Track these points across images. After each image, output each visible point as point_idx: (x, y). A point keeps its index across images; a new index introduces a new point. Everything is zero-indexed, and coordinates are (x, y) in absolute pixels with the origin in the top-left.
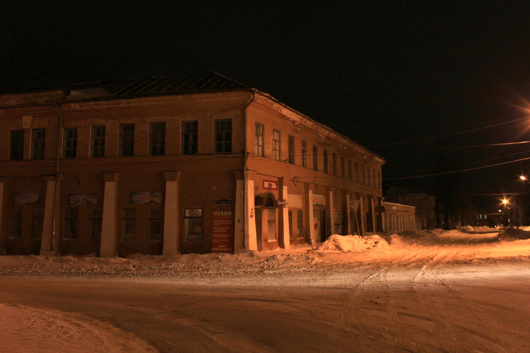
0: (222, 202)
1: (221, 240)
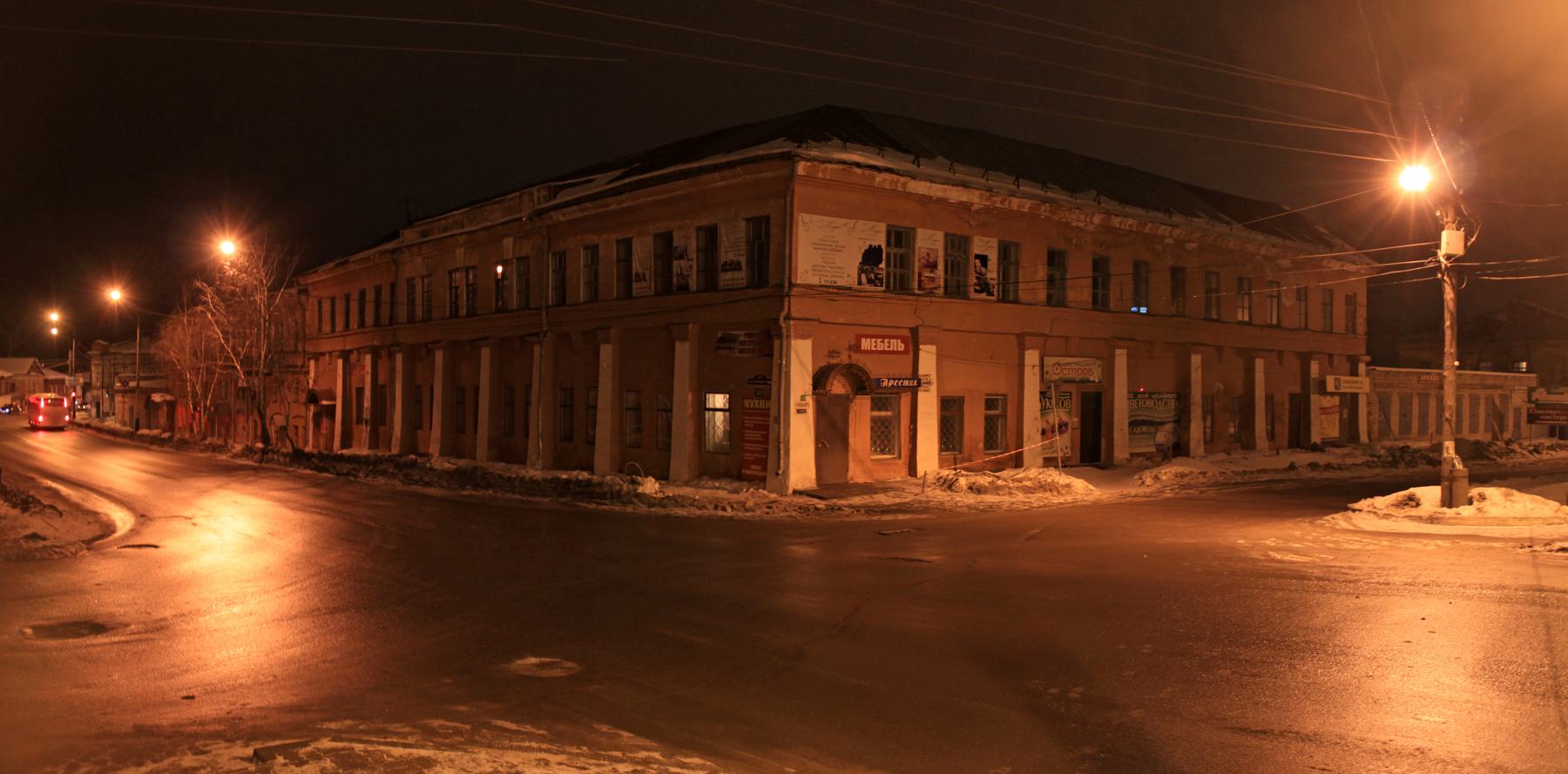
0: (757, 382)
1: (755, 455)
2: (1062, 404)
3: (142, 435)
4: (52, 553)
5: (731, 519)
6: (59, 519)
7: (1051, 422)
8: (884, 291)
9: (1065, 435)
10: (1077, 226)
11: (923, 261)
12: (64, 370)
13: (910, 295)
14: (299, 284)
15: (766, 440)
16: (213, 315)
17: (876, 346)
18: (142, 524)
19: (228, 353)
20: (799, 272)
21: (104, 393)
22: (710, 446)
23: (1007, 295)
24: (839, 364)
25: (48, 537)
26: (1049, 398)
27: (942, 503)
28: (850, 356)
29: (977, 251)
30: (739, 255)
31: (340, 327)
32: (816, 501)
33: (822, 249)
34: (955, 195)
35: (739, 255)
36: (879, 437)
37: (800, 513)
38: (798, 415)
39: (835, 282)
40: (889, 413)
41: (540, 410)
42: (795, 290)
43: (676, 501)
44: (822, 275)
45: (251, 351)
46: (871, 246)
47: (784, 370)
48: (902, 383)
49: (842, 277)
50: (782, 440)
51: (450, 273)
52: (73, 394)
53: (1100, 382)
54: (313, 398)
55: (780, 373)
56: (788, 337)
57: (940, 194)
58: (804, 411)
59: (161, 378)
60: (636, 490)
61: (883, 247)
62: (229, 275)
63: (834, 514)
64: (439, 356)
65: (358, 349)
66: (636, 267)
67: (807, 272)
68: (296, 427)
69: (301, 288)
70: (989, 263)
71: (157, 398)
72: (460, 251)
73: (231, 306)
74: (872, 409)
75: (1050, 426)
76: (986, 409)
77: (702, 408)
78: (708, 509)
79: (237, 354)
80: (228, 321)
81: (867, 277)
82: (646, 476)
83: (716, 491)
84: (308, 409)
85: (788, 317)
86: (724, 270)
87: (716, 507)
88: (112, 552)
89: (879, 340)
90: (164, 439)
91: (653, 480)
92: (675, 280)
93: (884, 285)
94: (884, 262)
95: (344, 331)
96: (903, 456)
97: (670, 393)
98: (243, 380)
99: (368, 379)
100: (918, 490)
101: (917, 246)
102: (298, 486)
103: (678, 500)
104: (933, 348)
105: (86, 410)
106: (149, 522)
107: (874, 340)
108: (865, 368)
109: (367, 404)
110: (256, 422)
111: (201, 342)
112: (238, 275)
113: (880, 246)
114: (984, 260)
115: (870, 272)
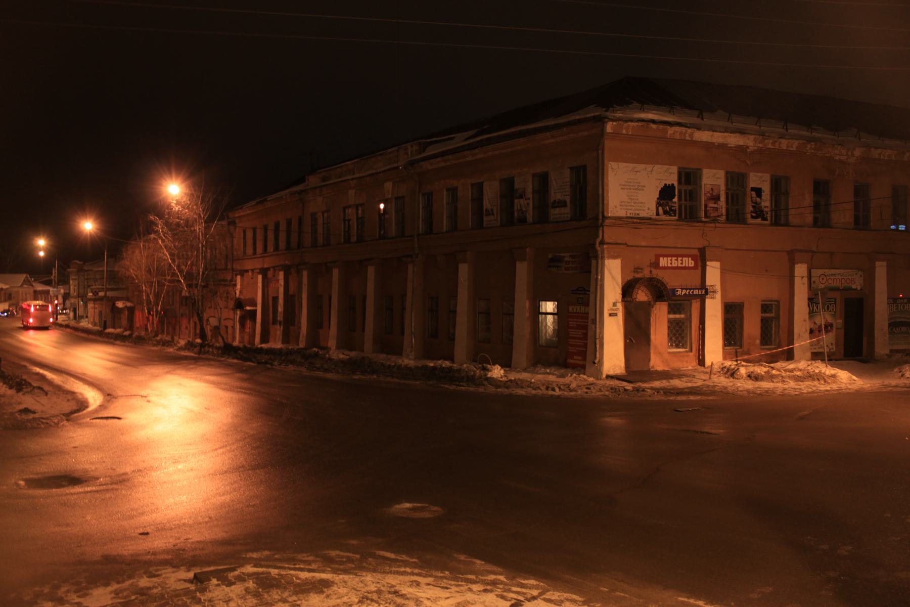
0: (579, 292)
1: (577, 348)
2: (828, 307)
3: (109, 333)
4: (40, 423)
5: (559, 397)
6: (45, 397)
7: (818, 322)
9: (831, 333)
10: (840, 159)
11: (708, 194)
12: (48, 283)
13: (698, 222)
14: (228, 218)
15: (586, 335)
16: (163, 241)
17: (671, 264)
18: (108, 401)
19: (174, 270)
20: (609, 207)
21: (79, 300)
22: (542, 341)
23: (779, 218)
24: (642, 278)
25: (36, 411)
26: (816, 304)
27: (726, 388)
28: (651, 271)
29: (752, 184)
30: (564, 195)
31: (260, 250)
32: (625, 384)
33: (627, 189)
34: (734, 140)
35: (564, 195)
36: (675, 335)
37: (612, 392)
38: (610, 317)
39: (638, 214)
40: (683, 316)
41: (413, 314)
42: (607, 222)
43: (517, 383)
44: (629, 209)
45: (192, 268)
46: (665, 185)
47: (599, 283)
48: (693, 292)
49: (644, 210)
50: (597, 337)
51: (344, 209)
52: (56, 302)
53: (861, 289)
54: (239, 304)
55: (596, 285)
56: (603, 258)
57: (721, 141)
58: (616, 315)
59: (123, 289)
60: (486, 375)
61: (676, 185)
62: (175, 211)
63: (639, 394)
64: (336, 273)
65: (274, 267)
66: (487, 204)
67: (616, 207)
68: (227, 327)
69: (231, 220)
70: (763, 194)
71: (120, 304)
72: (351, 193)
73: (176, 234)
74: (669, 313)
75: (817, 327)
76: (762, 313)
77: (536, 312)
78: (541, 390)
79: (181, 271)
80: (174, 246)
81: (663, 209)
82: (494, 364)
83: (547, 376)
84: (235, 313)
85: (602, 243)
86: (554, 207)
87: (547, 388)
88: (86, 423)
89: (674, 259)
90: (125, 336)
91: (499, 367)
92: (516, 214)
93: (677, 215)
94: (676, 197)
95: (263, 253)
96: (694, 350)
97: (512, 300)
98: (186, 291)
99: (281, 290)
100: (706, 377)
101: (703, 183)
102: (227, 372)
103: (519, 383)
104: (717, 264)
105: (65, 314)
106: (114, 400)
107: (669, 259)
108: (664, 281)
109: (280, 309)
110: (195, 323)
111: (154, 261)
112: (182, 210)
113: (673, 184)
114: (758, 191)
115: (666, 206)
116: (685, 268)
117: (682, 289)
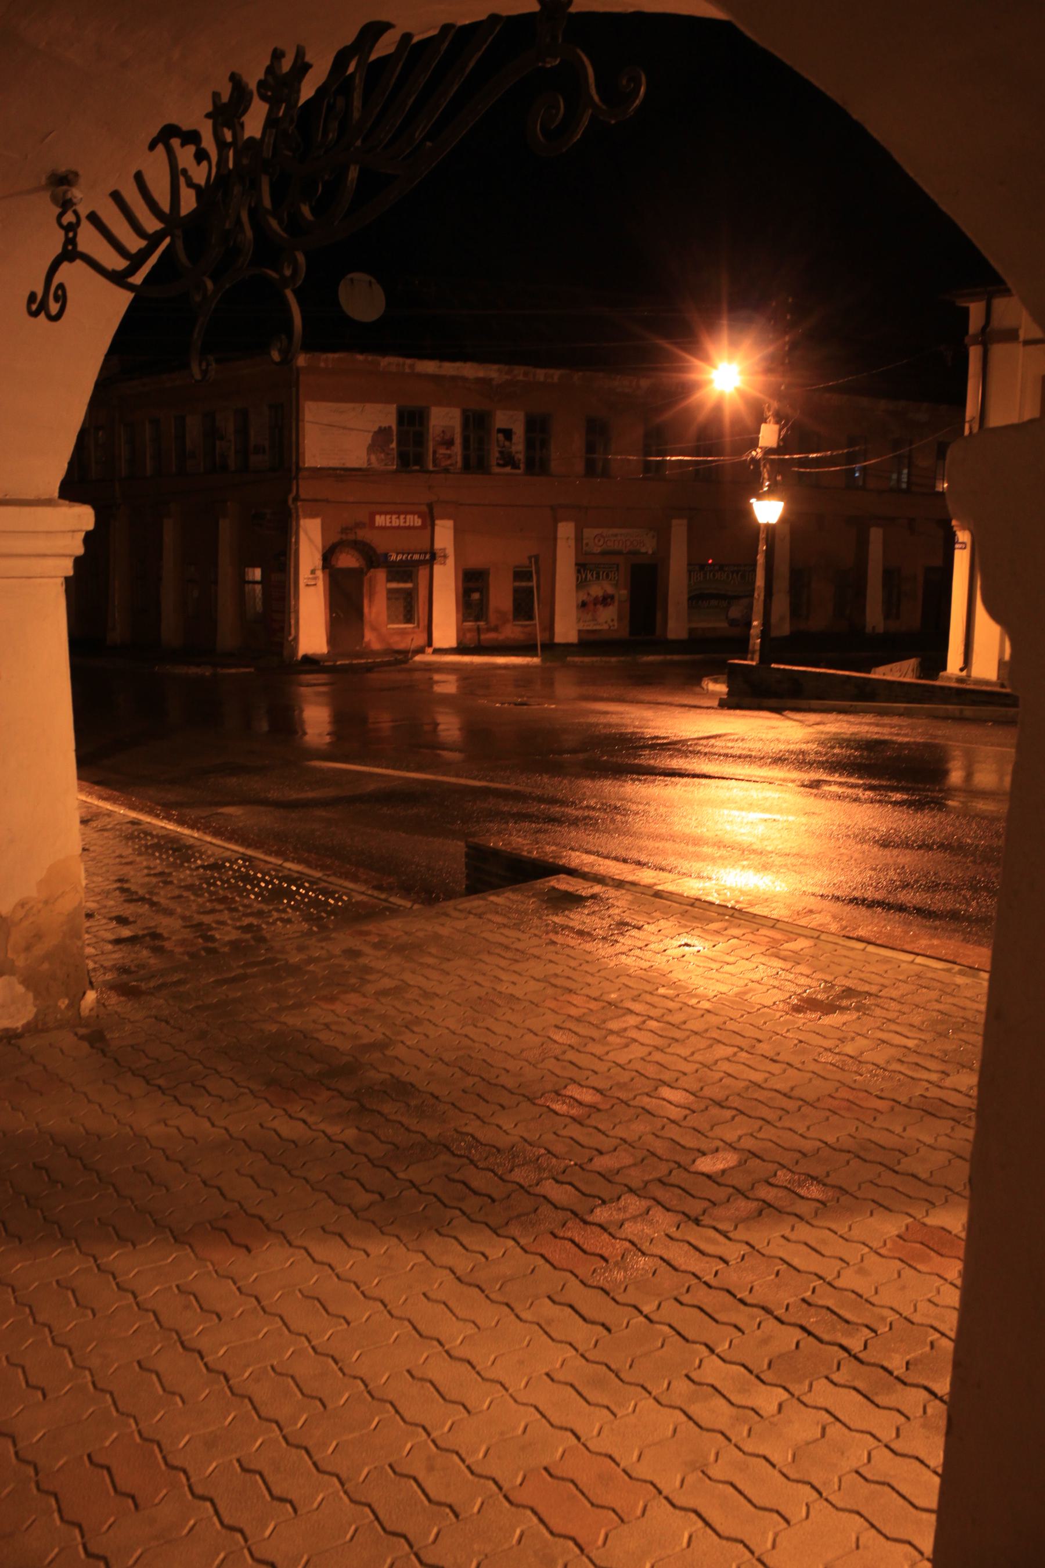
2: (607, 575)
8: (396, 472)
9: (611, 607)
11: (438, 439)
46: (380, 428)
53: (653, 553)
56: (298, 517)
77: (242, 581)
85: (296, 499)
89: (394, 517)
96: (421, 625)
104: (450, 523)
107: (388, 517)
113: (390, 427)
114: (508, 434)
116: (409, 528)
117: (398, 554)
